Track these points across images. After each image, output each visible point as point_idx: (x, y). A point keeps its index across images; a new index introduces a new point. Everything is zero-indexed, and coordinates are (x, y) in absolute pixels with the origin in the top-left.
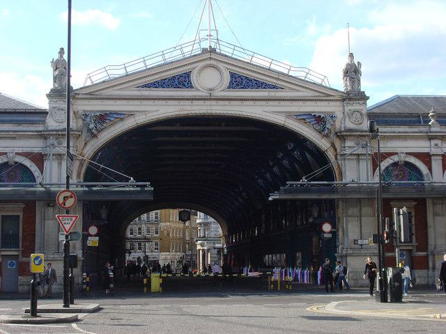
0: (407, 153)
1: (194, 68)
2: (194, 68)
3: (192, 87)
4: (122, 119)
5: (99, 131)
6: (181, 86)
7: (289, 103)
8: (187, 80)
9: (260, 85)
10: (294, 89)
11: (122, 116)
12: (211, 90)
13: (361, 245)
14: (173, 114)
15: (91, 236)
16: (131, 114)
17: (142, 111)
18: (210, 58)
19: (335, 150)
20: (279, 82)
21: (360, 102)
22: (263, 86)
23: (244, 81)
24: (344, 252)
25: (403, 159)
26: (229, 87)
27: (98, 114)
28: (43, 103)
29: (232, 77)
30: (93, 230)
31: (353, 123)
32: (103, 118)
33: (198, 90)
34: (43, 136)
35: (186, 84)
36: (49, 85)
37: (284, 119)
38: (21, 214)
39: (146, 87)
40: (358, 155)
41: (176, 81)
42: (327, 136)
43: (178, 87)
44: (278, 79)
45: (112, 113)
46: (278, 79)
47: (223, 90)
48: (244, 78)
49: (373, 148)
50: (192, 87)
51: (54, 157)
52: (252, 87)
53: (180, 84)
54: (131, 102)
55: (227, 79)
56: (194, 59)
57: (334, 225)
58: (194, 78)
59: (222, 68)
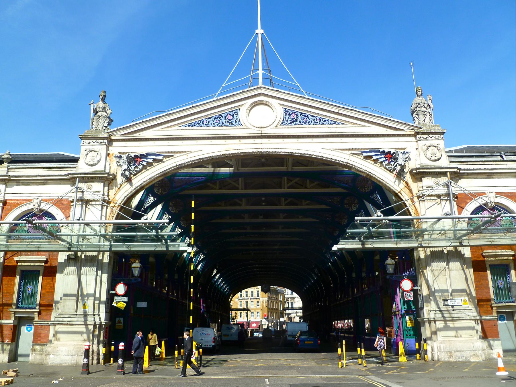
0: (498, 193)
4: (160, 161)
6: (228, 124)
9: (318, 121)
10: (357, 124)
11: (161, 157)
13: (453, 307)
15: (119, 296)
17: (183, 152)
18: (260, 94)
19: (411, 191)
21: (436, 136)
22: (322, 121)
23: (299, 117)
24: (432, 316)
25: (493, 200)
30: (121, 289)
31: (429, 159)
33: (247, 128)
34: (71, 180)
35: (234, 123)
37: (347, 157)
39: (189, 126)
40: (439, 196)
41: (223, 119)
42: (400, 175)
45: (148, 154)
48: (299, 114)
55: (280, 113)
57: (414, 281)
58: (243, 113)
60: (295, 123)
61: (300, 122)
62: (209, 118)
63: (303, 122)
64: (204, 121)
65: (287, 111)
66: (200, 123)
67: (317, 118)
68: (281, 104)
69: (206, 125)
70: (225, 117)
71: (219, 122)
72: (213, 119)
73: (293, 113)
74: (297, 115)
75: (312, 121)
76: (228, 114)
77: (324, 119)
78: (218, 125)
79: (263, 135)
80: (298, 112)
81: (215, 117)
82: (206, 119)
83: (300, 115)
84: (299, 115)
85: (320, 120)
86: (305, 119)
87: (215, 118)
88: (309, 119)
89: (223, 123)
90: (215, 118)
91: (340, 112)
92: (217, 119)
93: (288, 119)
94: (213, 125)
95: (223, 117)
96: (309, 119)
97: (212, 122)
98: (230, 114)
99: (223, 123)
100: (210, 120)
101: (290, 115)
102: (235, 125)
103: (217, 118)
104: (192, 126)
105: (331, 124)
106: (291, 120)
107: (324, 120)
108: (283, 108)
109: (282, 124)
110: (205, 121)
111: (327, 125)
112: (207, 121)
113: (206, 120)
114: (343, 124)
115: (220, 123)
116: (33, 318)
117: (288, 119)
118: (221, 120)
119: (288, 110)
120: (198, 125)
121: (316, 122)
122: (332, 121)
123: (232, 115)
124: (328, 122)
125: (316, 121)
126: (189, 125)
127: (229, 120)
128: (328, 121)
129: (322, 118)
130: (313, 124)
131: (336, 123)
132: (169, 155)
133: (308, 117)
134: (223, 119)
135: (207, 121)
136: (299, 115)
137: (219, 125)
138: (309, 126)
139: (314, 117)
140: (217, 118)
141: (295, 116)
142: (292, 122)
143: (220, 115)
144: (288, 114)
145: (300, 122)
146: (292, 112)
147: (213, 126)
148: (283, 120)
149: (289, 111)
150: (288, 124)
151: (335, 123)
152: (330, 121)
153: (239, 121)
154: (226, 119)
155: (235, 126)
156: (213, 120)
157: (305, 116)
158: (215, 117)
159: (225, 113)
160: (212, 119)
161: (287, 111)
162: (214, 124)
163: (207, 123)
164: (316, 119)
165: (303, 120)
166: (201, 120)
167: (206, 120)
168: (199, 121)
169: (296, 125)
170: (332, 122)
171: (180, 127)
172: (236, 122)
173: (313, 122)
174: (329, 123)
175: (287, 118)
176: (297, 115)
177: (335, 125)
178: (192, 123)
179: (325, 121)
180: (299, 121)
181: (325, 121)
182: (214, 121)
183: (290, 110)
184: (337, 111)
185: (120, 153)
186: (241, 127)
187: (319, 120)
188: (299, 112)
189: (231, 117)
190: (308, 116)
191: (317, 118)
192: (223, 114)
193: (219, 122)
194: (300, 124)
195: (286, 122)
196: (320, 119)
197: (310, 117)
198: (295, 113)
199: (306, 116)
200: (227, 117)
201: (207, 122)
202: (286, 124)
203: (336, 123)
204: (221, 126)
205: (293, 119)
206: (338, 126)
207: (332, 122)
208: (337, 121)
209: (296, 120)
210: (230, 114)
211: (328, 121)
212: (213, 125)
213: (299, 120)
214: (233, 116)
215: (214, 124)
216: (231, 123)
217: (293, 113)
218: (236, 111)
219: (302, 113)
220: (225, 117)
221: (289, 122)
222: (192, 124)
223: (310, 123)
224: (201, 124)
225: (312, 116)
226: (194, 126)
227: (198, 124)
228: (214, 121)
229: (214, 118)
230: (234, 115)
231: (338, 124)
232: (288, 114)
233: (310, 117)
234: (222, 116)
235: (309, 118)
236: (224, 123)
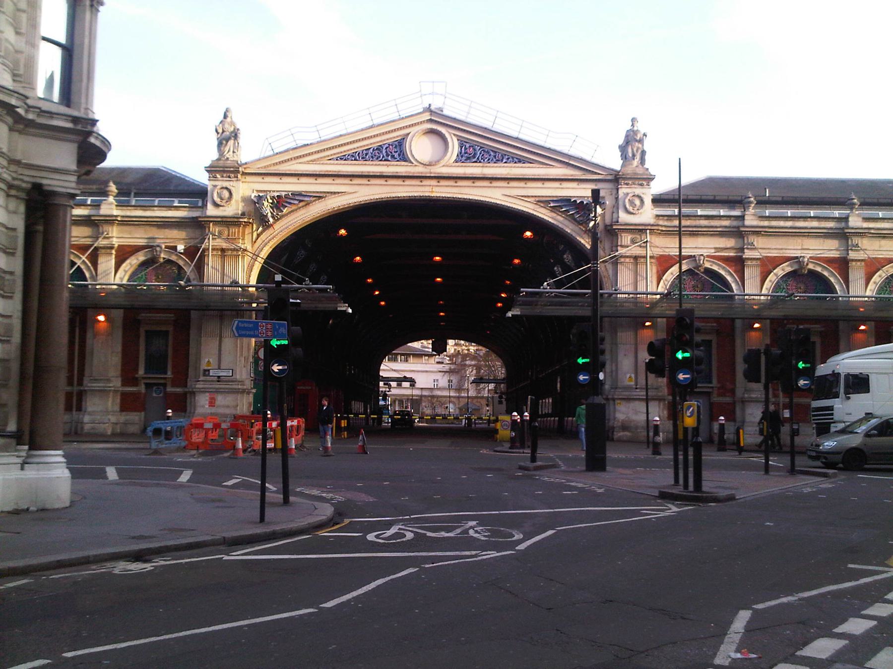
5: (276, 220)
7: (539, 184)
9: (499, 157)
14: (378, 197)
16: (319, 197)
18: (431, 121)
26: (456, 161)
27: (276, 194)
28: (201, 177)
32: (279, 203)
35: (396, 155)
36: (212, 155)
38: (171, 329)
39: (341, 159)
43: (385, 160)
45: (294, 194)
49: (668, 246)
51: (215, 253)
53: (388, 155)
54: (320, 180)
55: (454, 147)
56: (408, 122)
59: (447, 135)
61: (478, 158)
66: (354, 157)
88: (490, 155)
90: (373, 150)
95: (384, 148)
99: (383, 157)
102: (398, 159)
104: (345, 160)
107: (507, 157)
110: (361, 152)
114: (531, 163)
116: (165, 385)
118: (381, 152)
132: (319, 197)
133: (488, 152)
142: (468, 158)
143: (380, 146)
145: (478, 158)
154: (386, 152)
155: (398, 161)
166: (356, 152)
171: (330, 160)
172: (399, 155)
179: (508, 159)
185: (257, 191)
198: (472, 146)
205: (470, 154)
206: (524, 165)
217: (470, 147)
219: (481, 148)
220: (386, 148)
221: (464, 158)
223: (490, 161)
227: (353, 156)
229: (372, 149)
231: (524, 163)
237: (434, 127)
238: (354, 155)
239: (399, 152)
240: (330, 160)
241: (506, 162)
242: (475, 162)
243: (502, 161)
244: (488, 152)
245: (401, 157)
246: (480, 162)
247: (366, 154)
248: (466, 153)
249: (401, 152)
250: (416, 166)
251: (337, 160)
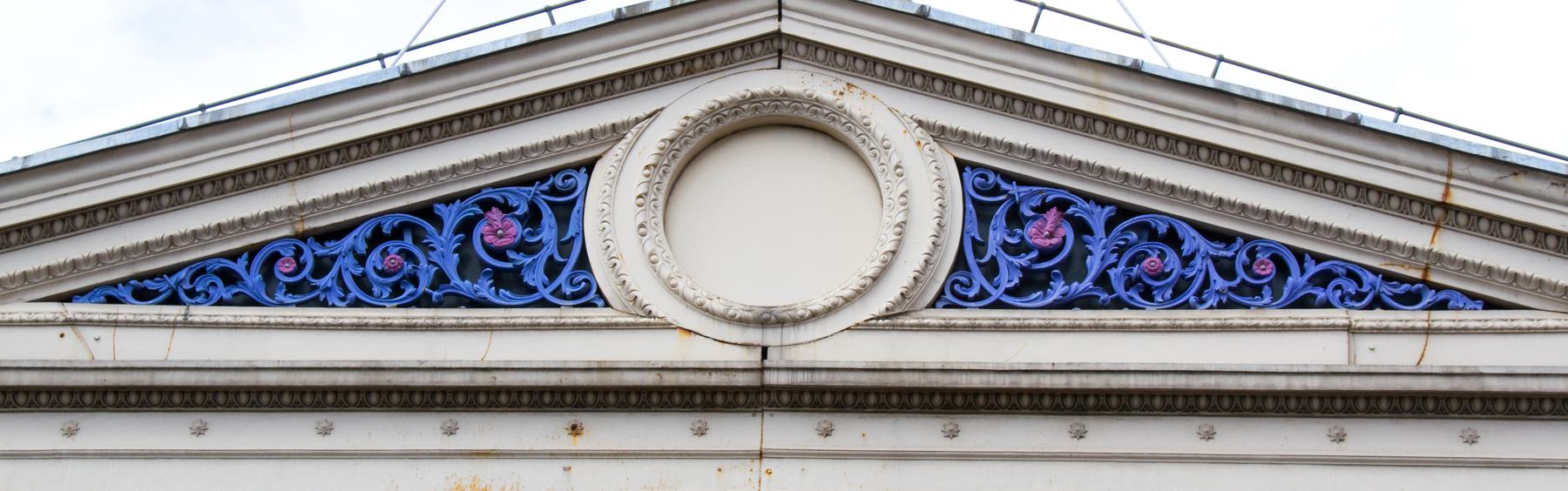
1: (616, 132)
2: (616, 132)
3: (587, 295)
6: (484, 289)
8: (548, 232)
12: (768, 320)
20: (1457, 246)
22: (1295, 279)
26: (953, 294)
29: (980, 209)
35: (535, 277)
39: (142, 295)
41: (444, 242)
44: (1441, 214)
46: (1441, 214)
47: (891, 320)
50: (587, 295)
52: (1181, 293)
60: (1059, 289)
61: (1103, 280)
62: (324, 236)
63: (1130, 284)
64: (276, 257)
65: (996, 190)
67: (1252, 254)
68: (941, 134)
69: (293, 289)
70: (467, 227)
71: (408, 267)
72: (356, 240)
73: (1042, 209)
74: (1081, 228)
75: (1214, 275)
76: (487, 205)
77: (1318, 258)
78: (397, 290)
79: (773, 379)
80: (1087, 197)
81: (378, 229)
82: (303, 236)
83: (1110, 225)
84: (1099, 226)
85: (1283, 270)
86: (1152, 262)
87: (376, 238)
88: (1187, 261)
89: (441, 278)
90: (376, 238)
91: (1460, 198)
92: (393, 247)
93: (1004, 260)
94: (355, 292)
96: (1187, 261)
97: (348, 264)
98: (506, 208)
99: (441, 278)
100: (332, 248)
101: (1015, 218)
102: (546, 293)
103: (397, 234)
104: (173, 300)
105: (1377, 303)
106: (1023, 261)
107: (1312, 269)
108: (961, 165)
109: (953, 294)
110: (288, 253)
111: (1338, 316)
112: (308, 257)
113: (299, 252)
114: (1490, 304)
115: (415, 281)
117: (1004, 260)
119: (1008, 177)
120: (226, 293)
121: (1240, 290)
122: (1388, 277)
123: (523, 209)
124: (1351, 288)
125: (1242, 275)
126: (150, 284)
127: (499, 254)
128: (1351, 275)
129: (1300, 255)
130: (1212, 301)
131: (1429, 297)
133: (1173, 239)
134: (444, 242)
135: (308, 257)
136: (1099, 226)
137: (410, 289)
138: (1184, 317)
139: (1226, 238)
140: (397, 234)
141: (1067, 231)
142: (1031, 282)
144: (1001, 212)
145: (1103, 280)
146: (1036, 202)
147: (357, 303)
148: (960, 263)
149: (1013, 189)
150: (996, 294)
151: (1410, 299)
152: (1368, 278)
153: (583, 262)
154: (464, 249)
155: (543, 303)
156: (362, 247)
157: (1153, 235)
158: (378, 229)
159: (463, 196)
160: (348, 241)
161: (996, 190)
162: (362, 282)
163: (306, 272)
164: (1243, 257)
165: (1133, 262)
166: (253, 251)
167: (299, 252)
168: (234, 256)
169: (1065, 304)
170: (1386, 290)
172: (553, 269)
173: (1219, 283)
174: (1359, 296)
175: (992, 250)
176: (1081, 228)
177: (1415, 317)
178: (172, 271)
179: (1324, 278)
180: (1092, 275)
181: (1324, 278)
182: (362, 260)
183: (1023, 181)
184: (1434, 192)
186: (596, 315)
187: (1270, 269)
188: (1102, 202)
189: (516, 230)
190: (1172, 231)
191: (1252, 254)
192: (448, 200)
193: (408, 267)
194: (1104, 296)
195: (979, 279)
196: (1278, 261)
197: (1193, 241)
198: (1062, 205)
199: (1162, 229)
200: (481, 228)
201: (301, 267)
202: (977, 298)
203: (1429, 297)
204: (423, 301)
205: (1046, 254)
206: (1443, 318)
207: (1386, 290)
208: (1435, 278)
209: (1072, 268)
210: (506, 208)
211: (1351, 275)
212: (362, 292)
213: (1094, 265)
214: (533, 218)
215: (362, 282)
216: (511, 282)
218: (558, 181)
219: (1124, 211)
220: (467, 227)
222: (172, 281)
224: (254, 279)
225: (1210, 233)
226: (192, 293)
227: (229, 277)
228: (362, 260)
229: (366, 231)
230: (547, 212)
231: (1442, 305)
232: (1001, 212)
233: (1193, 241)
234: (438, 222)
235: (1186, 248)
236: (451, 271)
237: (793, 80)
238: (239, 266)
239: (550, 249)
240: (66, 298)
241: (1305, 303)
242: (1087, 302)
243: (1276, 296)
244: (1173, 239)
245: (562, 279)
246: (1119, 304)
247: (321, 268)
248: (1021, 248)
249: (565, 246)
250: (667, 326)
251: (111, 300)
